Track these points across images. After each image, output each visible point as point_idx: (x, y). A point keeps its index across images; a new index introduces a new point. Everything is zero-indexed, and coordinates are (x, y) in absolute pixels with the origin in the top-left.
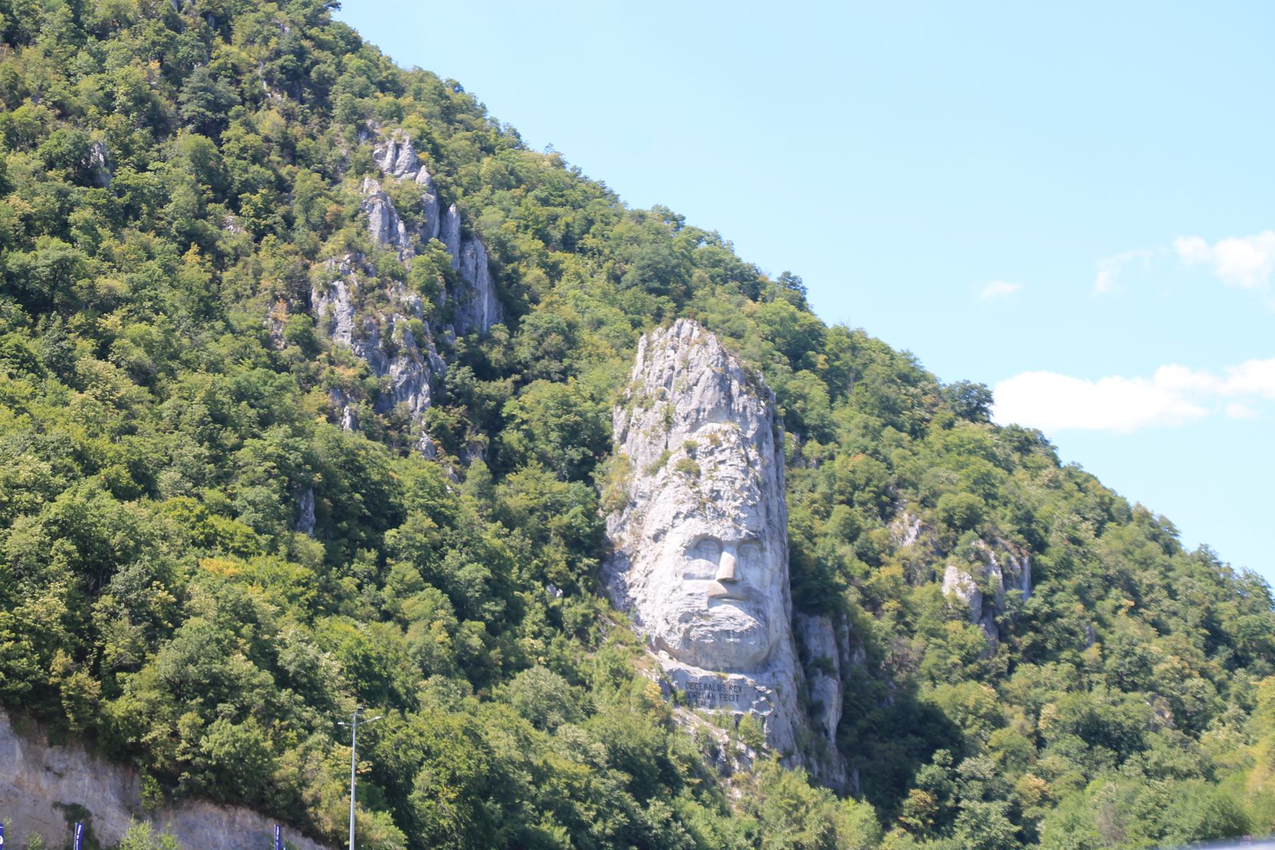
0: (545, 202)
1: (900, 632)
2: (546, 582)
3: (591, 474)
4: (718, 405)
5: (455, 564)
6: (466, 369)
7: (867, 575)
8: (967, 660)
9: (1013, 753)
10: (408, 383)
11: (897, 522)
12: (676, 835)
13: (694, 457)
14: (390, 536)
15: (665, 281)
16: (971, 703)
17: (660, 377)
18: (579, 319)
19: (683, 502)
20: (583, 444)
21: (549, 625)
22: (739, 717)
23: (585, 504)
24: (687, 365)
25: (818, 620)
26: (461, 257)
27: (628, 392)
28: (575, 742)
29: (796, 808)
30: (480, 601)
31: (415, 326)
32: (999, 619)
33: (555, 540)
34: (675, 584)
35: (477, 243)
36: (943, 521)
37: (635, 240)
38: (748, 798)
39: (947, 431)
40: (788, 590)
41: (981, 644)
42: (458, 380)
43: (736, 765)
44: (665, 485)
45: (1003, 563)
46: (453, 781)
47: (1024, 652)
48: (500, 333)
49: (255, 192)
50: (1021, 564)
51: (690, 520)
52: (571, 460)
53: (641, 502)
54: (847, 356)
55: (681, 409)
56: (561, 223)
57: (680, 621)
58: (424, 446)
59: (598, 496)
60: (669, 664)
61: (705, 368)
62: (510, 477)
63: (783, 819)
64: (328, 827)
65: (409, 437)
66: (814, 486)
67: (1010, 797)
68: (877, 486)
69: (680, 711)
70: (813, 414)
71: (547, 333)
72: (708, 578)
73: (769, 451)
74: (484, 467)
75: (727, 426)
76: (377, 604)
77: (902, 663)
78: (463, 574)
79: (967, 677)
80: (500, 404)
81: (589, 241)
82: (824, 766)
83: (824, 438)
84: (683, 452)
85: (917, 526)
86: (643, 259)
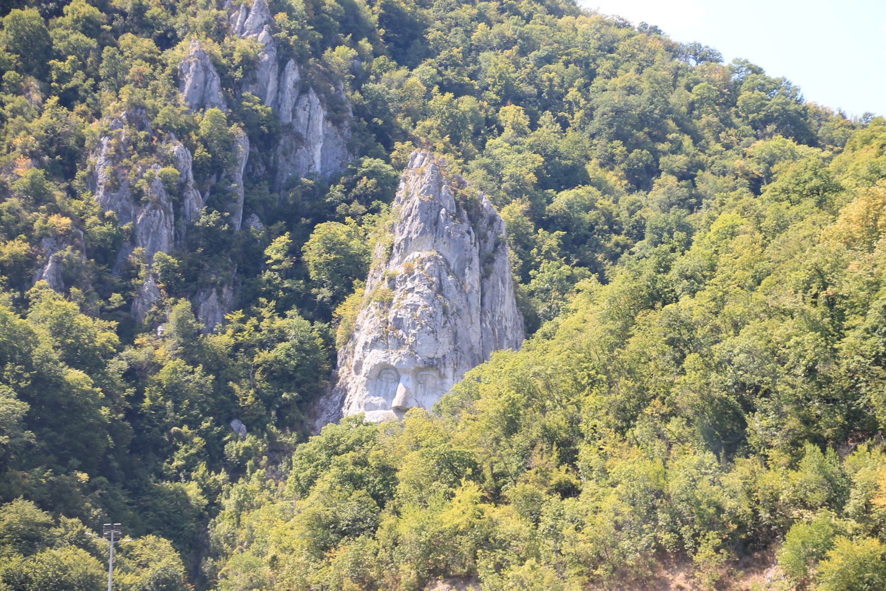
0: (549, 59)
26: (294, 111)
33: (258, 376)
49: (63, 59)
51: (375, 351)
55: (398, 238)
73: (472, 278)
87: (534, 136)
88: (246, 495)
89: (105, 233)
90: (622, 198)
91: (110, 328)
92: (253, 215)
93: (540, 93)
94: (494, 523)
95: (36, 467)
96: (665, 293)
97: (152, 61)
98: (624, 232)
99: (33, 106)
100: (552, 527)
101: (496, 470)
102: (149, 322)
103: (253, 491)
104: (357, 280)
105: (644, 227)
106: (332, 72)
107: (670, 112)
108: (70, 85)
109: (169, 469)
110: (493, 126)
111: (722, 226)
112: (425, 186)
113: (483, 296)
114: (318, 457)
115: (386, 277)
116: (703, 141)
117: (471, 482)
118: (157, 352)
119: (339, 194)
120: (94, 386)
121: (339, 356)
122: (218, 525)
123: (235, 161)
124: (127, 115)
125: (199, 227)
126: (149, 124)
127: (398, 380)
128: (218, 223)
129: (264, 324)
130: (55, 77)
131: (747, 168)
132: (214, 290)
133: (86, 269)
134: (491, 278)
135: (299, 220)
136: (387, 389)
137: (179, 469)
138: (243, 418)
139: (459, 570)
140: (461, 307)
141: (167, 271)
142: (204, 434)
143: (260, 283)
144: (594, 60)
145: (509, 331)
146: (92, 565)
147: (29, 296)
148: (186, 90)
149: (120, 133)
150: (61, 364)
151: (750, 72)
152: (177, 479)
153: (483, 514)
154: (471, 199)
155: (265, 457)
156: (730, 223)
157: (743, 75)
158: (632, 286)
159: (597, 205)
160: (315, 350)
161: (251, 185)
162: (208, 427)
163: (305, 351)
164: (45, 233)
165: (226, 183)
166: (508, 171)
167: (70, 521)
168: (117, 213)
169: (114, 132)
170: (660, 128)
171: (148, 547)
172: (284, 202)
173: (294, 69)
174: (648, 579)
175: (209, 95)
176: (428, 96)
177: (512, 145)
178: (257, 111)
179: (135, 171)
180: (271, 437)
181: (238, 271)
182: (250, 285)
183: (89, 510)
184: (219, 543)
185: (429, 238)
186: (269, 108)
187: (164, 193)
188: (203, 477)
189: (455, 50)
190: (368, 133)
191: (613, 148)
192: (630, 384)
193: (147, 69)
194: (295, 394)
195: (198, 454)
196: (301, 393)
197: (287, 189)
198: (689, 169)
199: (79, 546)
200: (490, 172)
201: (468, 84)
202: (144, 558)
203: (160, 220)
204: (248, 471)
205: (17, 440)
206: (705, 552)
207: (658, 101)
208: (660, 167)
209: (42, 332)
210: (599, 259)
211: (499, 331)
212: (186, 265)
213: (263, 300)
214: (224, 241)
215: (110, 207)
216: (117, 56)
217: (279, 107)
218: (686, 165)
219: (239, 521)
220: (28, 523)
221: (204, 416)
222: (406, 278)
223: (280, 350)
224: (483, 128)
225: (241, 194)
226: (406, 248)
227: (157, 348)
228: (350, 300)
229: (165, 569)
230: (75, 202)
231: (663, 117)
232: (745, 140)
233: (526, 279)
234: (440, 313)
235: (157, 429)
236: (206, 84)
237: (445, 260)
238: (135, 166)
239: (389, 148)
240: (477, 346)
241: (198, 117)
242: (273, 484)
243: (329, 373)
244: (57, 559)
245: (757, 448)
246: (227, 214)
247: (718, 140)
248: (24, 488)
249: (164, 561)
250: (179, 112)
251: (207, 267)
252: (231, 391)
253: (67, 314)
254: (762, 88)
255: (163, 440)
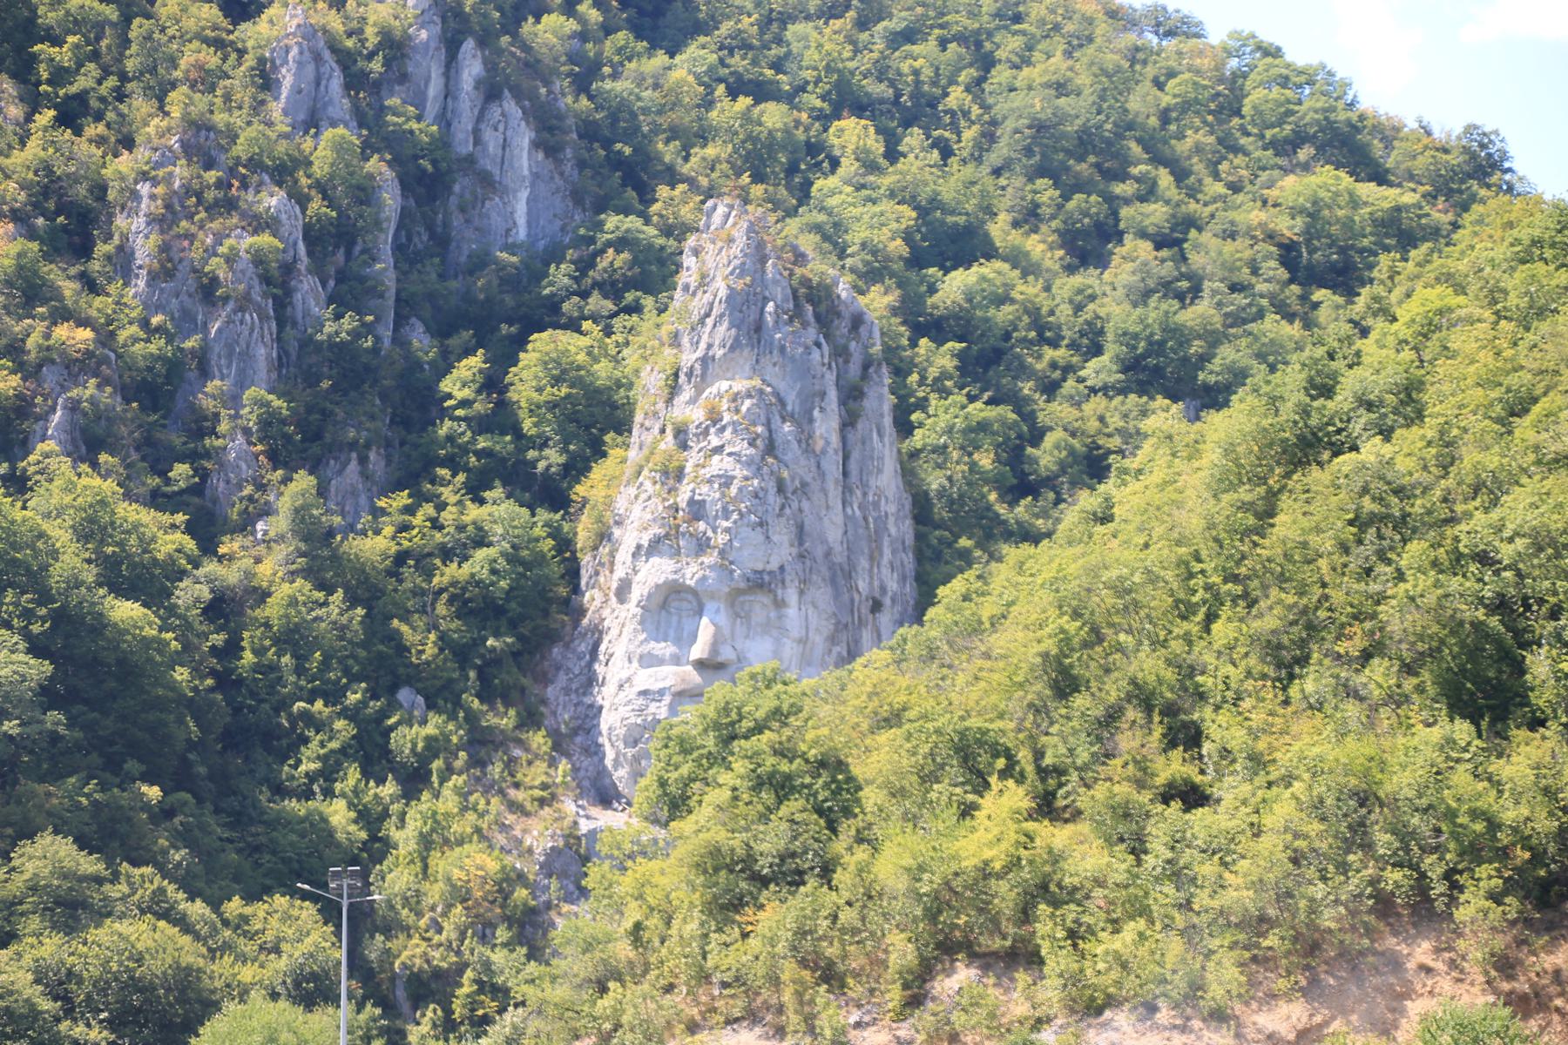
0: (909, 36)
26: (476, 133)
33: (441, 609)
34: (624, 675)
49: (57, 42)
51: (655, 560)
55: (689, 358)
70: (1216, 364)
73: (826, 426)
87: (895, 173)
88: (436, 822)
89: (152, 355)
90: (1058, 282)
91: (174, 526)
92: (413, 320)
93: (898, 95)
94: (1055, 858)
95: (70, 775)
96: (1328, 434)
97: (218, 44)
98: (1066, 342)
99: (10, 128)
100: (1169, 862)
101: (1048, 761)
102: (239, 514)
103: (447, 815)
104: (612, 434)
105: (1101, 332)
106: (538, 61)
107: (1130, 126)
108: (73, 89)
109: (293, 777)
110: (819, 157)
111: (1421, 310)
112: (737, 262)
113: (846, 458)
114: (699, 742)
115: (669, 430)
116: (1192, 179)
117: (1011, 783)
118: (260, 568)
119: (566, 280)
120: (161, 630)
121: (583, 572)
122: (389, 877)
123: (377, 223)
124: (181, 141)
125: (322, 342)
126: (223, 157)
127: (700, 612)
128: (356, 334)
129: (448, 516)
130: (45, 76)
131: (1272, 226)
132: (354, 455)
133: (123, 421)
134: (860, 426)
135: (499, 329)
136: (680, 628)
137: (311, 777)
138: (420, 685)
139: (997, 944)
140: (808, 479)
141: (269, 422)
142: (351, 714)
143: (434, 441)
144: (990, 35)
145: (891, 520)
146: (189, 952)
147: (25, 470)
148: (283, 96)
149: (171, 174)
150: (102, 592)
151: (1258, 55)
152: (308, 795)
153: (1032, 839)
154: (819, 284)
155: (462, 754)
156: (1438, 304)
157: (1247, 59)
158: (1265, 423)
159: (1015, 294)
160: (540, 559)
161: (406, 267)
162: (359, 702)
163: (522, 563)
164: (48, 356)
165: (365, 262)
166: (857, 236)
167: (137, 872)
168: (172, 319)
169: (161, 173)
170: (1115, 156)
171: (276, 916)
172: (468, 297)
173: (474, 56)
174: (1361, 953)
175: (325, 106)
176: (708, 103)
177: (858, 189)
178: (411, 132)
179: (203, 243)
180: (472, 719)
181: (392, 421)
182: (416, 446)
183: (165, 852)
184: (392, 907)
185: (746, 356)
186: (435, 128)
187: (256, 282)
188: (356, 792)
189: (746, 20)
190: (605, 171)
191: (1035, 192)
192: (1290, 599)
193: (212, 59)
194: (509, 640)
195: (343, 751)
196: (521, 638)
197: (471, 273)
198: (1172, 230)
199: (159, 916)
200: (826, 238)
201: (771, 82)
202: (269, 936)
203: (252, 330)
204: (435, 778)
205: (35, 727)
206: (1471, 907)
207: (1110, 107)
208: (1122, 225)
209: (60, 534)
210: (1026, 391)
211: (875, 520)
212: (302, 410)
213: (443, 472)
214: (368, 369)
215: (159, 308)
216: (156, 36)
217: (449, 125)
218: (1167, 221)
219: (426, 867)
220: (65, 876)
221: (350, 681)
222: (707, 428)
223: (478, 563)
224: (803, 160)
225: (390, 282)
226: (703, 375)
227: (258, 561)
228: (599, 471)
229: (311, 955)
230: (98, 301)
231: (1120, 136)
232: (1264, 176)
233: (905, 428)
234: (772, 490)
235: (266, 706)
236: (318, 84)
237: (776, 394)
238: (201, 235)
239: (647, 197)
240: (838, 548)
241: (308, 144)
242: (482, 802)
243: (566, 602)
244: (125, 939)
245: (1549, 711)
246: (370, 318)
247: (1216, 176)
248: (49, 814)
249: (308, 940)
250: (273, 136)
251: (340, 414)
252: (394, 638)
253: (103, 503)
254: (1284, 82)
255: (280, 725)
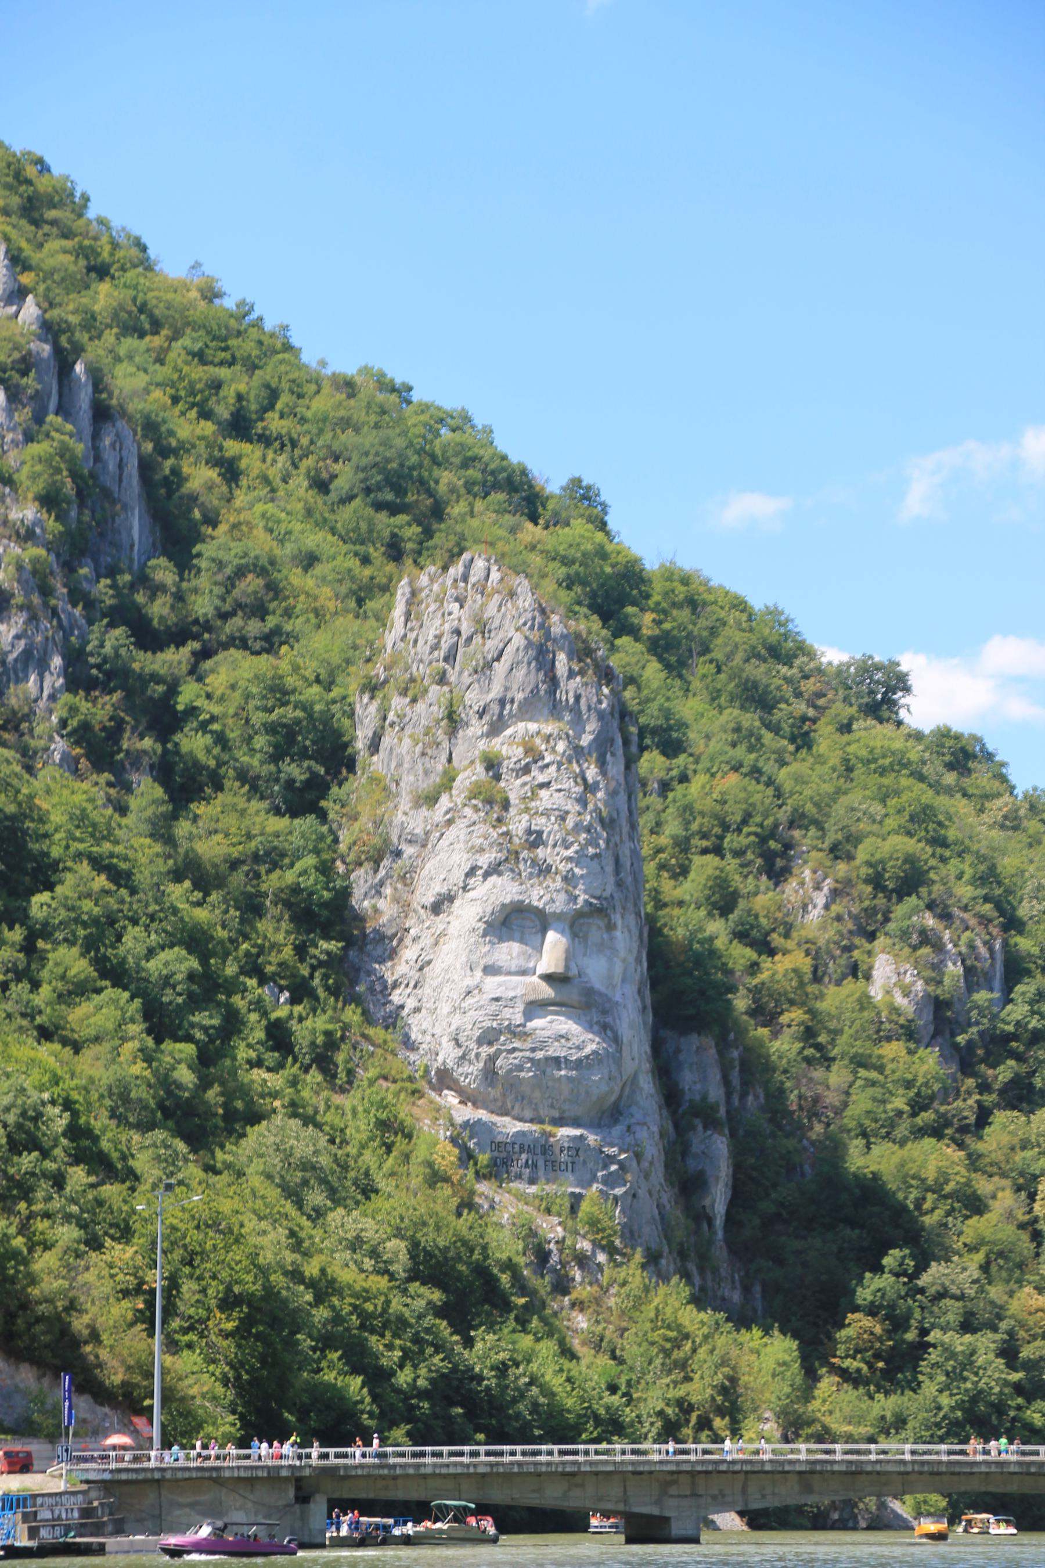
1: (808, 1061)
2: (263, 981)
3: (323, 803)
4: (535, 692)
5: (141, 949)
6: (119, 632)
7: (754, 968)
8: (918, 1106)
9: (1001, 1254)
10: (27, 654)
11: (793, 883)
12: (517, 1389)
13: (498, 777)
14: (40, 904)
15: (400, 491)
16: (930, 1174)
17: (436, 647)
18: (278, 552)
19: (482, 850)
20: (304, 755)
21: (273, 1049)
22: (576, 1200)
23: (317, 852)
24: (483, 628)
25: (694, 1040)
27: (379, 671)
28: (358, 1237)
29: (678, 1345)
30: (182, 1011)
31: (35, 561)
32: (961, 1039)
34: (470, 982)
35: (121, 424)
36: (867, 881)
37: (346, 423)
38: (599, 1329)
39: (846, 738)
40: (647, 993)
41: (938, 1080)
42: (108, 649)
43: (577, 1275)
44: (450, 822)
45: (964, 949)
46: (228, 1302)
47: (1002, 1092)
48: (163, 571)
50: (991, 950)
51: (493, 879)
52: (290, 782)
53: (409, 851)
54: (683, 615)
55: (474, 698)
56: (229, 392)
57: (480, 1042)
58: (57, 757)
59: (336, 841)
60: (465, 1113)
61: (512, 632)
62: (199, 808)
63: (658, 1362)
64: (116, 1377)
65: (33, 743)
66: (658, 824)
67: (1003, 1325)
68: (761, 825)
69: (483, 1187)
71: (240, 572)
72: (523, 972)
73: (616, 767)
74: (159, 792)
75: (549, 728)
76: (30, 1013)
77: (814, 1108)
78: (154, 966)
79: (920, 1132)
80: (173, 690)
81: (274, 423)
82: (709, 1276)
83: (672, 747)
84: (480, 768)
85: (826, 890)
86: (367, 454)
127: (544, 931)
